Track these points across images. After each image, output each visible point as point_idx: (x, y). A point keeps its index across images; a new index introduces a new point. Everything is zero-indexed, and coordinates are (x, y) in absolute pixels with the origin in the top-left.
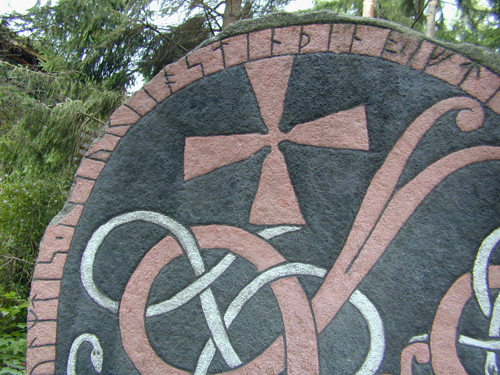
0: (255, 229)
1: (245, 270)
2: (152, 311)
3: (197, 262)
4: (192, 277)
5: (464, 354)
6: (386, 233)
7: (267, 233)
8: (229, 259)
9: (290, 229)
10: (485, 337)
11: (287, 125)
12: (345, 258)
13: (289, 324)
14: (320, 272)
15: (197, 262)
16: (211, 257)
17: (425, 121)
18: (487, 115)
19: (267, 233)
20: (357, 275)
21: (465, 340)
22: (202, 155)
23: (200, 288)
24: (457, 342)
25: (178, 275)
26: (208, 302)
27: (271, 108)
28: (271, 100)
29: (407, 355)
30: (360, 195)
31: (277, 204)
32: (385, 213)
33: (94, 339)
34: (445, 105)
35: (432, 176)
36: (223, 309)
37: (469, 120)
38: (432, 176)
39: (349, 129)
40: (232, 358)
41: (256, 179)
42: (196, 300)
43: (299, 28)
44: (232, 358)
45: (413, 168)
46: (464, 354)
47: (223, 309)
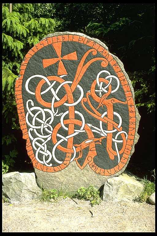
0: (59, 76)
1: (58, 84)
2: (42, 93)
3: (49, 84)
4: (48, 86)
5: (96, 93)
6: (82, 75)
7: (61, 77)
8: (55, 82)
9: (65, 75)
10: (99, 90)
11: (62, 56)
12: (75, 80)
13: (67, 92)
14: (71, 82)
15: (49, 84)
16: (51, 82)
17: (87, 53)
18: (97, 52)
19: (61, 77)
20: (78, 82)
21: (96, 91)
22: (47, 63)
23: (50, 88)
24: (95, 92)
25: (46, 86)
26: (52, 90)
27: (59, 53)
28: (59, 52)
29: (87, 94)
30: (77, 68)
31: (62, 71)
32: (81, 70)
33: (31, 100)
34: (90, 51)
35: (88, 64)
36: (55, 91)
37: (95, 53)
38: (88, 64)
39: (73, 56)
40: (58, 99)
41: (57, 67)
42: (50, 90)
43: (62, 36)
44: (58, 99)
45: (85, 63)
46: (96, 93)
47: (55, 91)
